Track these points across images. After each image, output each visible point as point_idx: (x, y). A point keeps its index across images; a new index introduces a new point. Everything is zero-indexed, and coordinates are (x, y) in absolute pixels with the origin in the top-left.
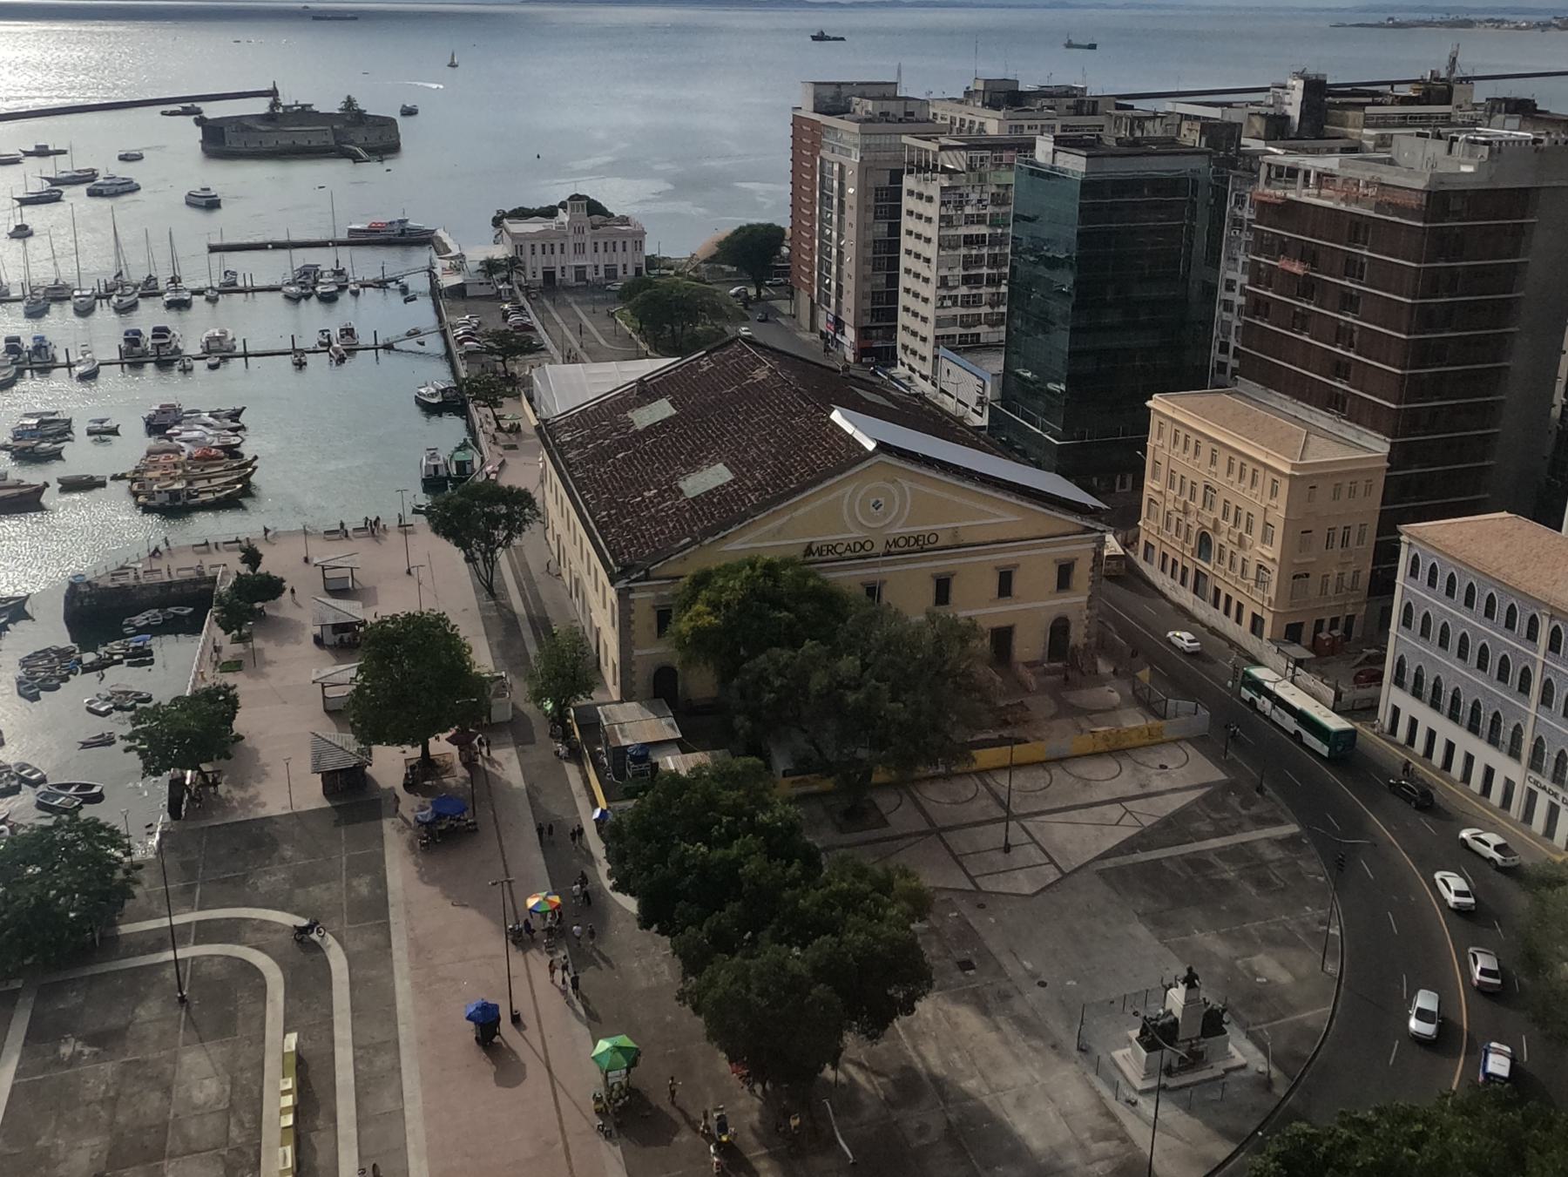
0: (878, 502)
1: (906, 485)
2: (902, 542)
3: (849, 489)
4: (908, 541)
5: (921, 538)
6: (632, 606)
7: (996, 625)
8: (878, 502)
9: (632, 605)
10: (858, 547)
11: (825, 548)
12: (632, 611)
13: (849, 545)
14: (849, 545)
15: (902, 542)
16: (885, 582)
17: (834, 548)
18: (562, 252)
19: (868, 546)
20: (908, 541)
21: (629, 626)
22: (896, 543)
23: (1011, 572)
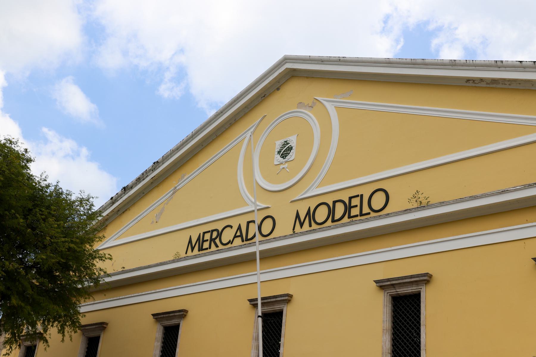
0: (286, 143)
4: (331, 211)
8: (286, 143)
13: (239, 228)
14: (239, 228)
15: (321, 214)
16: (287, 299)
17: (220, 235)
20: (331, 211)
22: (311, 215)
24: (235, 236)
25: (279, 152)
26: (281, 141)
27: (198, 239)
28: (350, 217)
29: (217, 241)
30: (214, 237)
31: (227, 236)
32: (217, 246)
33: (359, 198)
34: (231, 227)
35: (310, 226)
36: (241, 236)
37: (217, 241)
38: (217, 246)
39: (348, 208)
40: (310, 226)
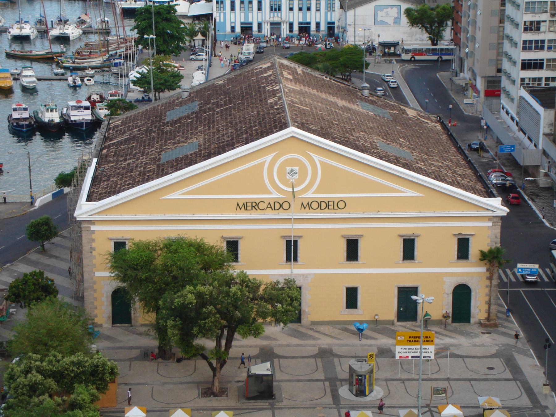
1: (317, 158)
2: (315, 205)
3: (268, 158)
4: (320, 205)
5: (330, 203)
6: (94, 236)
7: (402, 285)
9: (93, 235)
10: (277, 206)
11: (249, 204)
12: (93, 240)
13: (269, 203)
14: (269, 203)
15: (315, 205)
18: (260, 9)
19: (286, 206)
21: (91, 252)
22: (310, 205)
23: (414, 240)
24: (267, 207)
25: (289, 173)
26: (291, 168)
27: (244, 204)
28: (328, 209)
29: (256, 207)
30: (253, 205)
31: (261, 206)
32: (256, 210)
33: (333, 202)
34: (264, 202)
35: (309, 209)
36: (271, 207)
37: (256, 207)
38: (256, 210)
39: (327, 205)
40: (309, 209)
